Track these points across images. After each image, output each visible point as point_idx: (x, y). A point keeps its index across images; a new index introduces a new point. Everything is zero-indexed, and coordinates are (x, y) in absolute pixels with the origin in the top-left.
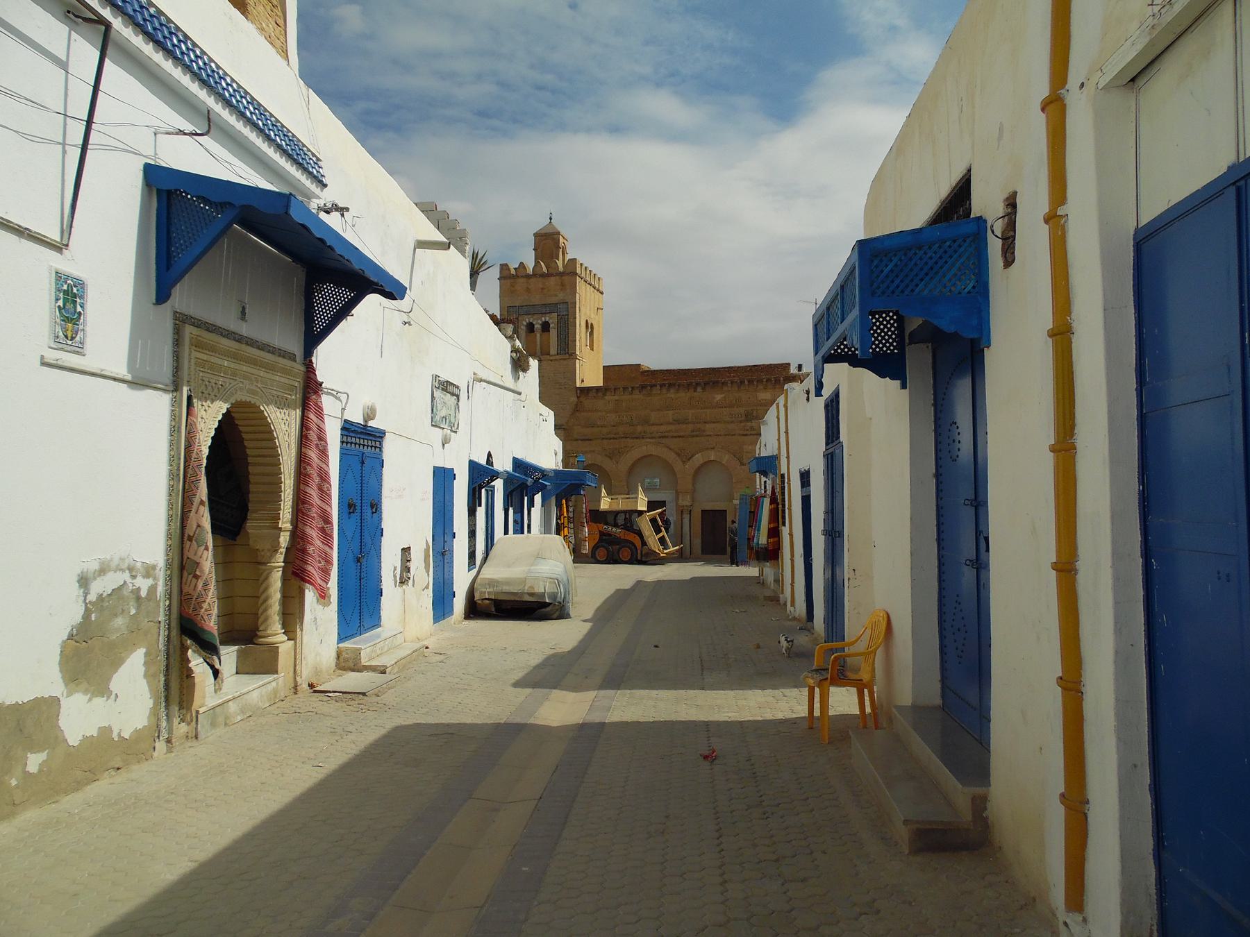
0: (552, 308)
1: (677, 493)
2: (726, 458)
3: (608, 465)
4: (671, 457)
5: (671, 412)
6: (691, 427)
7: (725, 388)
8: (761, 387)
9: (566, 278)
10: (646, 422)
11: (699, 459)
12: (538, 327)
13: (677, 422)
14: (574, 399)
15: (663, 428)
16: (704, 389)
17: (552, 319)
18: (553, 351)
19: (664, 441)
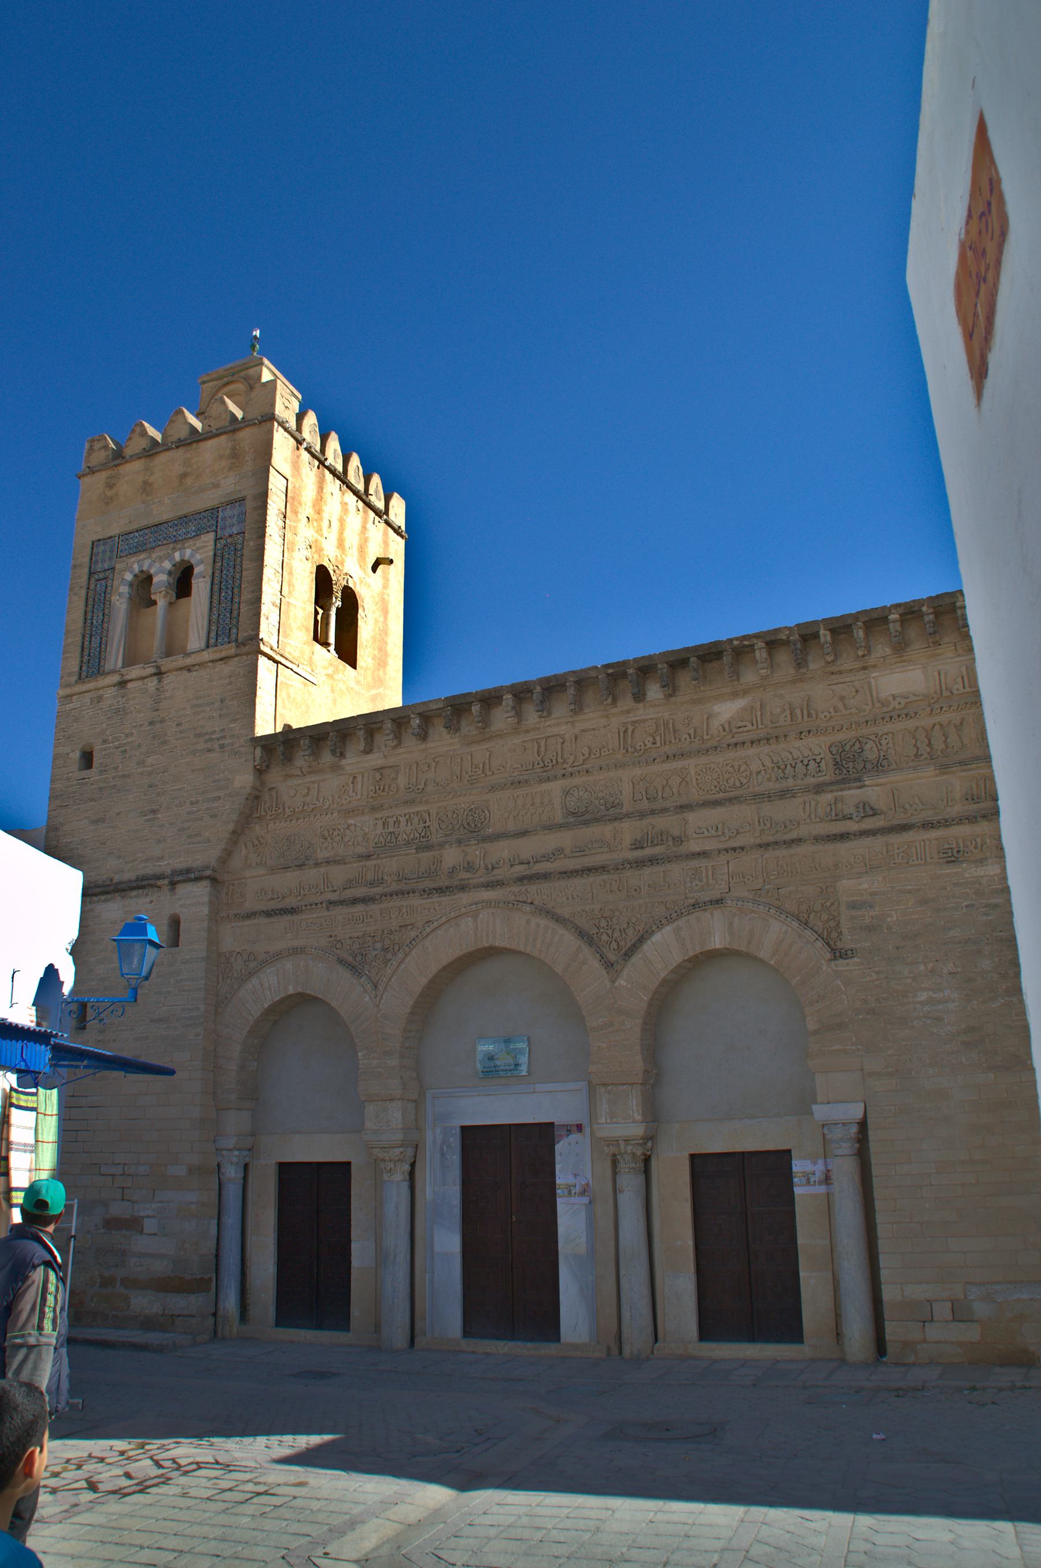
0: (208, 519)
1: (592, 1088)
2: (773, 935)
3: (344, 992)
4: (561, 947)
5: (555, 787)
6: (629, 830)
7: (749, 677)
8: (882, 649)
9: (245, 435)
10: (474, 829)
11: (664, 951)
12: (160, 579)
13: (580, 817)
14: (244, 780)
15: (529, 847)
16: (671, 689)
17: (199, 552)
18: (195, 640)
19: (535, 891)
